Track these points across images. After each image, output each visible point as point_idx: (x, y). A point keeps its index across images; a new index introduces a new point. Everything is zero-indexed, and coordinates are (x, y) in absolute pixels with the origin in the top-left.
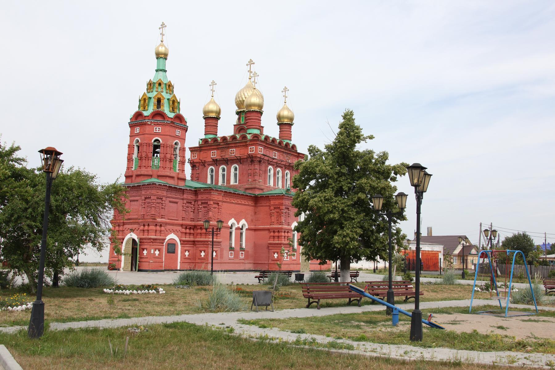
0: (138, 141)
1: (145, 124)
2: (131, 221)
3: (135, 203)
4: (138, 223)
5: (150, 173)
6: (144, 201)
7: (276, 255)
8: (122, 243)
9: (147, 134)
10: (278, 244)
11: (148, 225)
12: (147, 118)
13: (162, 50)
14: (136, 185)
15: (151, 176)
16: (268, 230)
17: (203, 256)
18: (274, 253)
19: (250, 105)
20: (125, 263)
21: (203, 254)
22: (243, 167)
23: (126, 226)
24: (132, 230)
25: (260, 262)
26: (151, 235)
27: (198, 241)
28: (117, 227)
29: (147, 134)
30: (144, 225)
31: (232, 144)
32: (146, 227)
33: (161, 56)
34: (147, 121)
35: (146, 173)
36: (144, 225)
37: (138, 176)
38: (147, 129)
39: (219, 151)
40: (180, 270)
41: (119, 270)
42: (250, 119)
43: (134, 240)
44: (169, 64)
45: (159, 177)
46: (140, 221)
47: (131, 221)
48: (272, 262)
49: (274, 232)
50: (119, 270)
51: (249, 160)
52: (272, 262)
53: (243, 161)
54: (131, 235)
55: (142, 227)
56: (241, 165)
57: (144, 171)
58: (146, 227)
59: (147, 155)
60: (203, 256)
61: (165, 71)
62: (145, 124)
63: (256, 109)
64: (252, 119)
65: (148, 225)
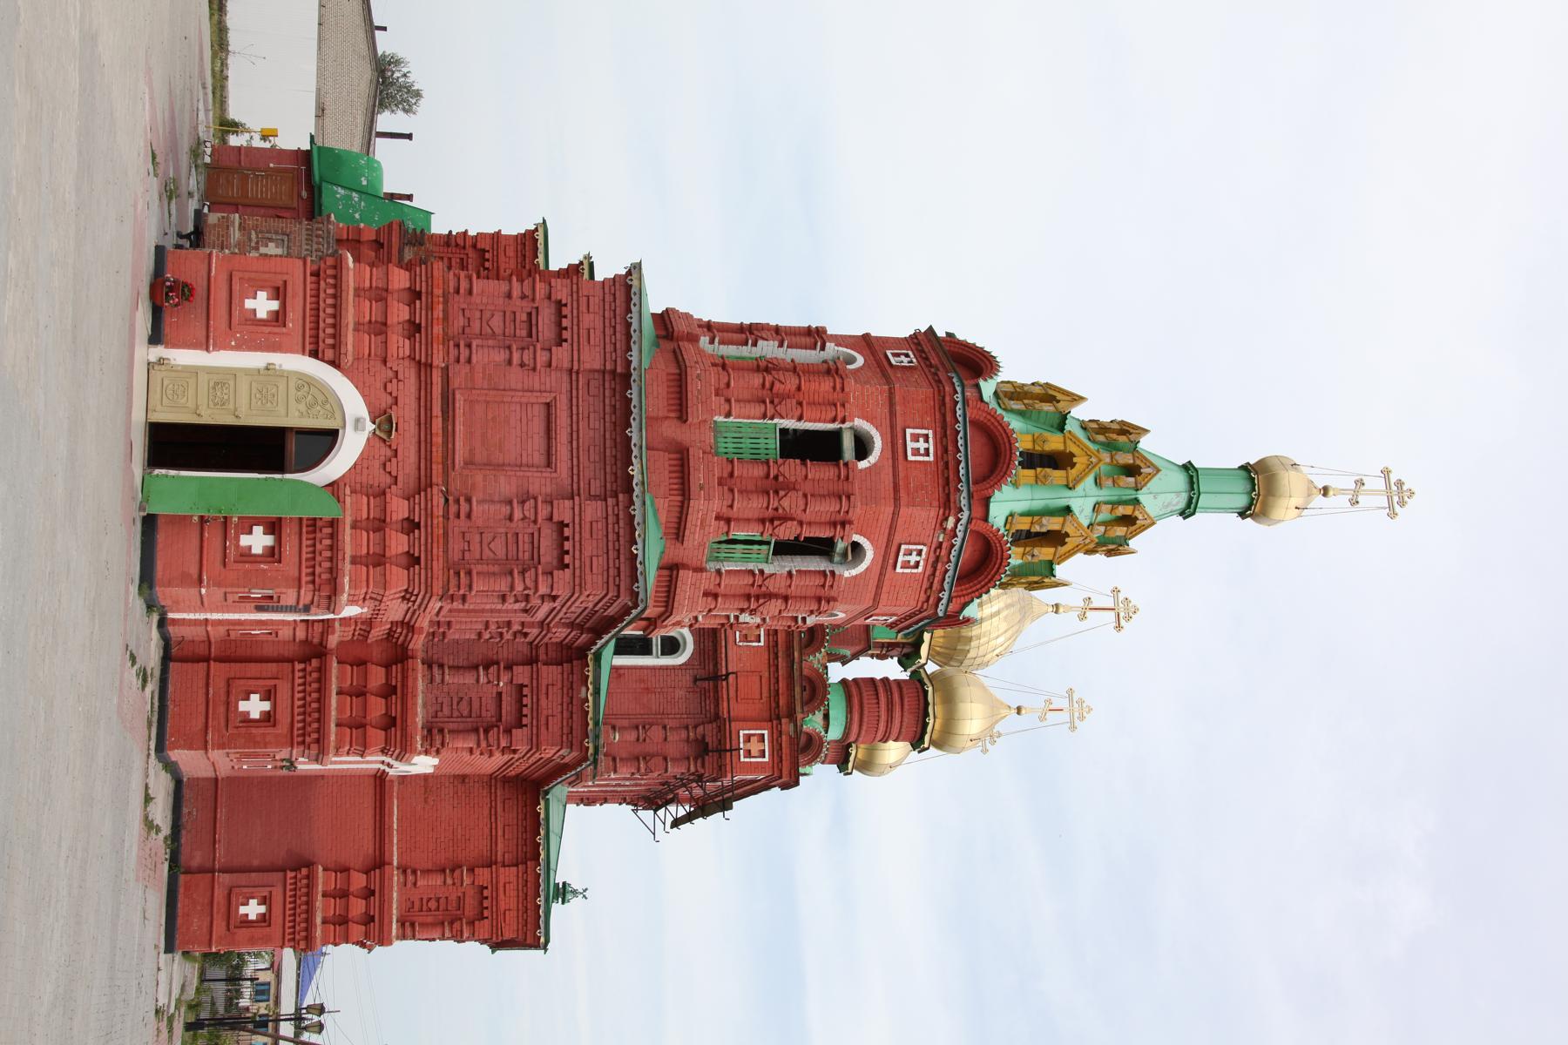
0: (862, 449)
1: (947, 505)
2: (437, 424)
3: (538, 442)
4: (423, 486)
5: (693, 535)
6: (543, 511)
7: (253, 910)
8: (315, 354)
9: (895, 514)
10: (309, 921)
11: (413, 560)
12: (978, 512)
13: (1292, 487)
14: (635, 470)
15: (677, 531)
16: (379, 863)
17: (243, 706)
18: (263, 901)
19: (950, 700)
20: (194, 371)
21: (255, 706)
22: (680, 693)
23: (409, 374)
24: (384, 419)
25: (222, 814)
26: (357, 306)
27: (322, 671)
28: (404, 313)
29: (895, 514)
30: (411, 526)
31: (790, 676)
32: (398, 543)
33: (1257, 488)
34: (965, 516)
35: (694, 518)
36: (411, 526)
37: (682, 459)
38: (921, 516)
39: (762, 664)
40: (162, 623)
41: (155, 338)
42: (890, 711)
43: (327, 439)
44: (1218, 526)
45: (671, 570)
46: (439, 500)
47: (437, 424)
48: (219, 894)
49: (368, 893)
50: (155, 338)
51: (709, 731)
52: (219, 894)
53: (704, 692)
54: (358, 422)
55: (399, 509)
56: (687, 679)
57: (704, 507)
58: (398, 543)
59: (790, 487)
60: (243, 706)
61: (1187, 512)
62: (947, 505)
63: (934, 724)
64: (890, 711)
65: (413, 560)
